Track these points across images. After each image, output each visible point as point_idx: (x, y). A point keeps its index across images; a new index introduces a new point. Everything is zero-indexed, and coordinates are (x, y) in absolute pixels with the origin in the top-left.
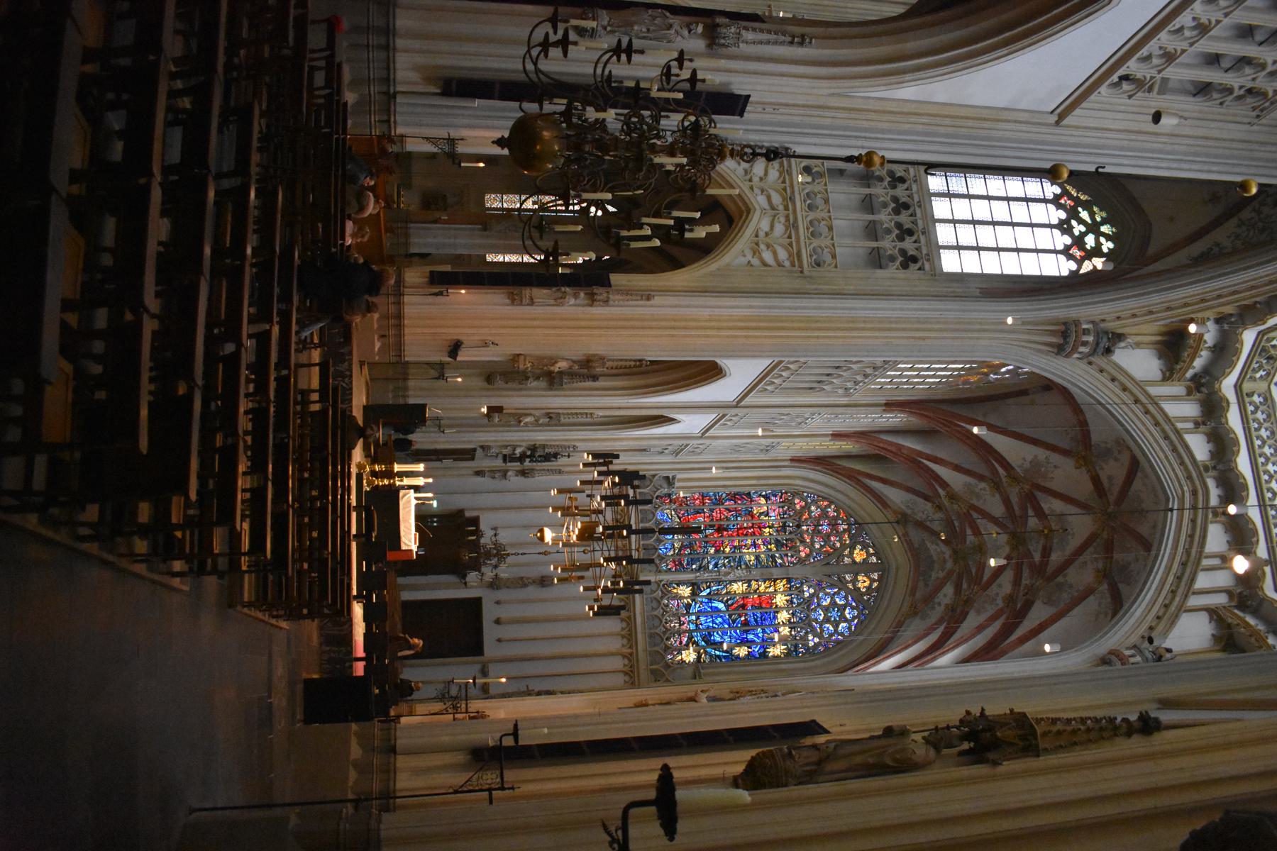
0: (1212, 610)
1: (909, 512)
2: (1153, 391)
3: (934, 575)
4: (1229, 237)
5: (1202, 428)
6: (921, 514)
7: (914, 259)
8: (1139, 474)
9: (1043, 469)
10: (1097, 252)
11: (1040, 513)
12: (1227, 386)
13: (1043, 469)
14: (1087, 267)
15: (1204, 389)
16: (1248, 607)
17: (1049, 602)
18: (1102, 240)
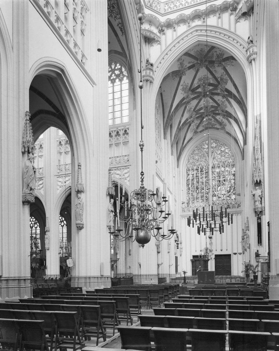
0: (236, 21)
1: (193, 131)
2: (164, 48)
3: (213, 122)
4: (115, 20)
5: (176, 29)
6: (194, 127)
7: (126, 131)
8: (189, 52)
9: (185, 87)
10: (120, 70)
11: (198, 87)
12: (163, 20)
14: (125, 73)
15: (163, 28)
16: (236, 7)
17: (226, 83)
18: (116, 68)
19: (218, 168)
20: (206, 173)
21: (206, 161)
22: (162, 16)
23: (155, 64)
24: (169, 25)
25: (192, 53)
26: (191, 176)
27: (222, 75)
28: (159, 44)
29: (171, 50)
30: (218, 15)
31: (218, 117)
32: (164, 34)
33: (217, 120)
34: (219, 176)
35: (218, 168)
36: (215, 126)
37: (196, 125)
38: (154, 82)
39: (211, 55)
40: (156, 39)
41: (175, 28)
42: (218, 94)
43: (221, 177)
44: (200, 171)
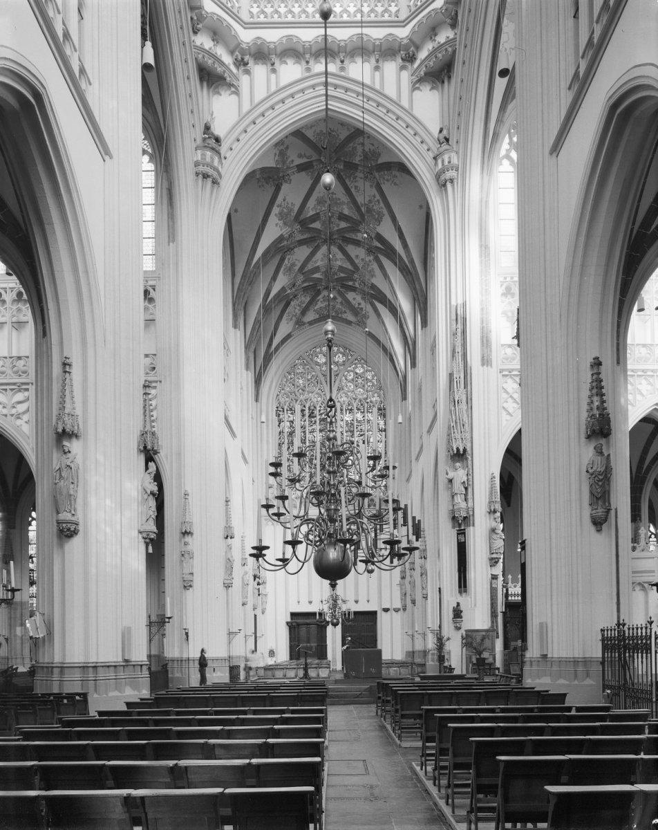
3: (339, 306)
6: (297, 311)
11: (315, 218)
12: (247, 36)
13: (285, 210)
15: (247, 58)
16: (414, 55)
17: (379, 221)
19: (350, 413)
20: (321, 420)
21: (322, 394)
22: (245, 28)
23: (226, 137)
24: (262, 54)
25: (310, 134)
26: (288, 424)
27: (370, 201)
28: (233, 93)
29: (264, 116)
30: (373, 60)
31: (350, 296)
32: (248, 72)
33: (348, 302)
34: (351, 431)
35: (348, 412)
36: (344, 316)
37: (299, 306)
38: (223, 183)
39: (350, 149)
40: (228, 79)
41: (274, 64)
42: (357, 243)
43: (356, 434)
44: (307, 415)
